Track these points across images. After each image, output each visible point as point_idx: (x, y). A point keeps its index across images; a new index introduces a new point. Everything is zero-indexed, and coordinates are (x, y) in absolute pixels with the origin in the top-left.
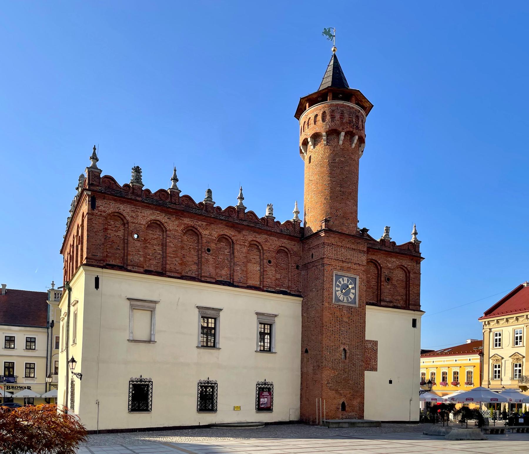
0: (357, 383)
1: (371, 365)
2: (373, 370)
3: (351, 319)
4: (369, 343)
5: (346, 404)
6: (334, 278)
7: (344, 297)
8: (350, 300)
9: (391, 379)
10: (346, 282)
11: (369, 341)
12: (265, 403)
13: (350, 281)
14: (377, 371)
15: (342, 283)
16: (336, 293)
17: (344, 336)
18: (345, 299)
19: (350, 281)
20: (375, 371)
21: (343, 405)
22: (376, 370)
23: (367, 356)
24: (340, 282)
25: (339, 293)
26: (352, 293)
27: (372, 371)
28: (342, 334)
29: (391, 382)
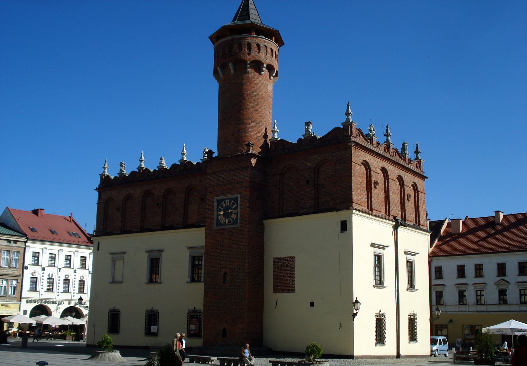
0: (239, 307)
1: (288, 285)
2: (291, 291)
3: (233, 241)
4: (285, 261)
5: (227, 331)
6: (216, 204)
7: (226, 219)
8: (232, 221)
9: (312, 300)
10: (228, 204)
11: (286, 258)
12: (194, 329)
13: (232, 202)
14: (295, 292)
15: (224, 206)
16: (217, 218)
17: (225, 259)
18: (227, 221)
19: (232, 202)
20: (293, 292)
21: (224, 330)
22: (293, 291)
23: (283, 275)
24: (222, 206)
25: (220, 218)
26: (234, 213)
27: (290, 292)
28: (223, 258)
29: (312, 304)
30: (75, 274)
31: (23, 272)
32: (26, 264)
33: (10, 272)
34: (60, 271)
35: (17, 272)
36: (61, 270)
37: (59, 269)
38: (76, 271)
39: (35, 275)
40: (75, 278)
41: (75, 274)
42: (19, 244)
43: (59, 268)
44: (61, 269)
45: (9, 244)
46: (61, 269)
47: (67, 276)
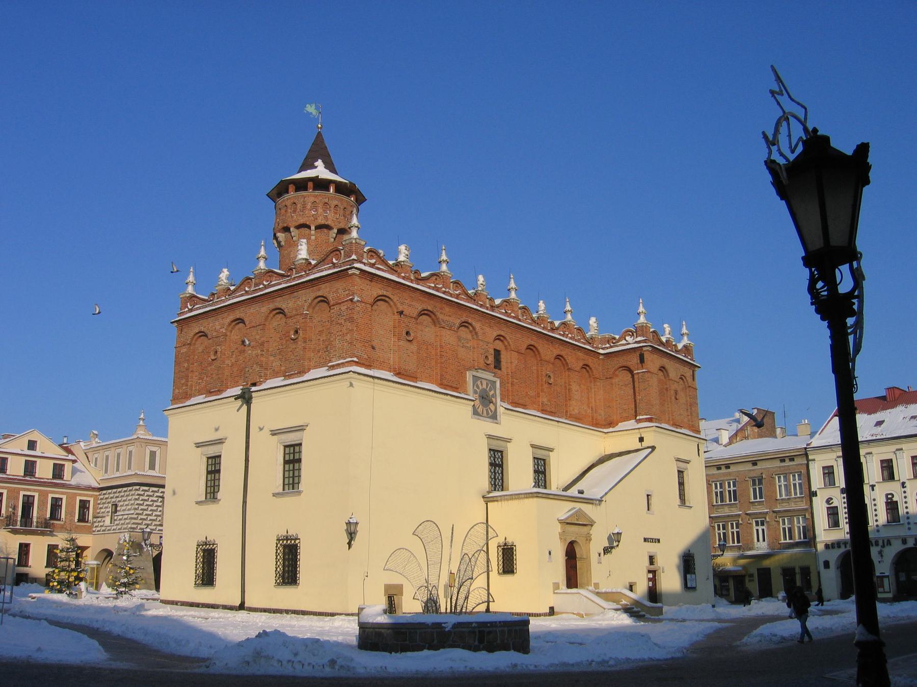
30: (905, 489)
31: (811, 501)
32: (813, 489)
33: (793, 506)
34: (873, 490)
35: (803, 505)
36: (874, 488)
37: (871, 486)
38: (906, 485)
39: (832, 503)
40: (905, 497)
41: (903, 490)
42: (798, 461)
43: (871, 484)
44: (875, 486)
45: (783, 464)
46: (875, 486)
47: (890, 496)
